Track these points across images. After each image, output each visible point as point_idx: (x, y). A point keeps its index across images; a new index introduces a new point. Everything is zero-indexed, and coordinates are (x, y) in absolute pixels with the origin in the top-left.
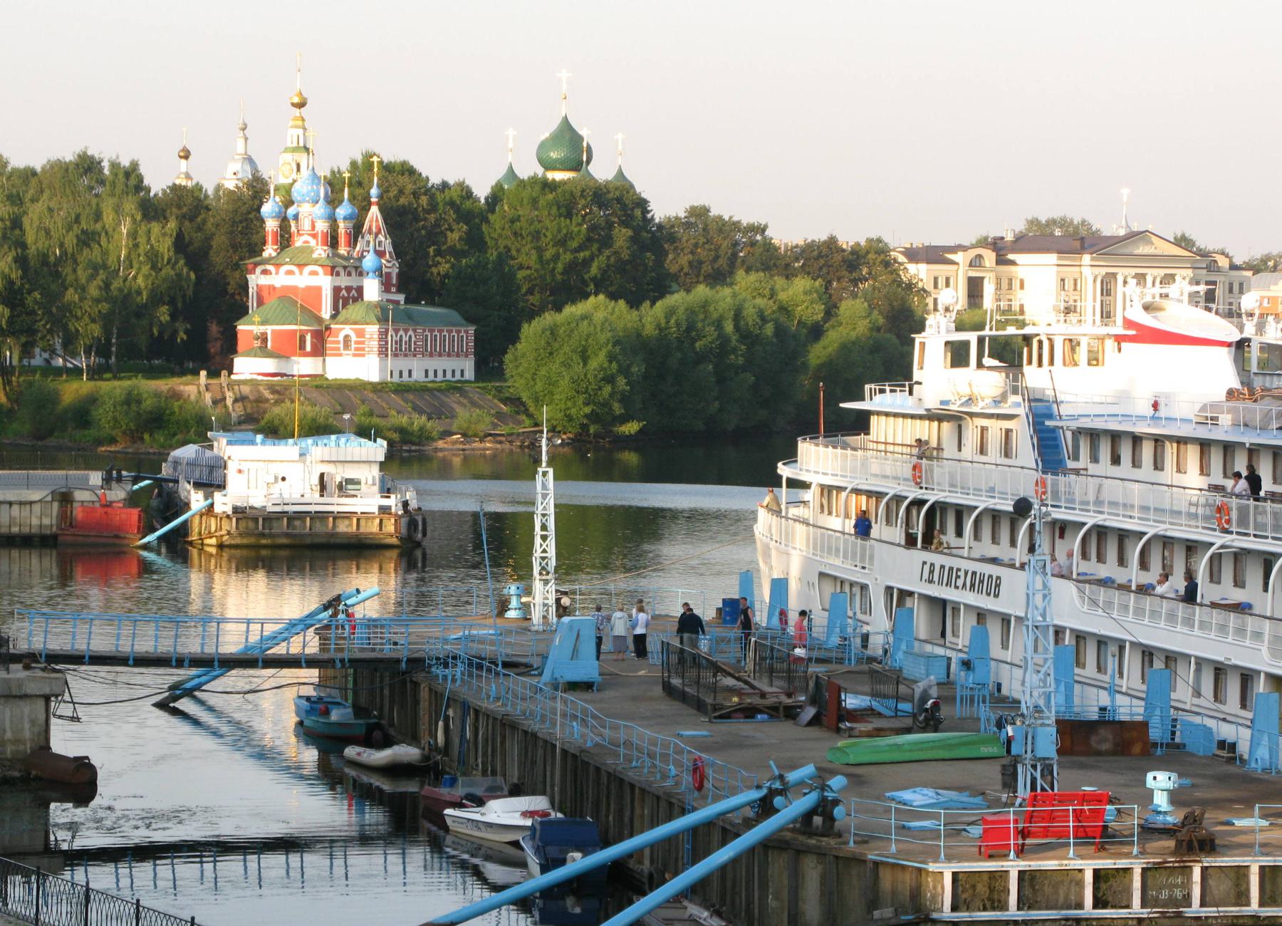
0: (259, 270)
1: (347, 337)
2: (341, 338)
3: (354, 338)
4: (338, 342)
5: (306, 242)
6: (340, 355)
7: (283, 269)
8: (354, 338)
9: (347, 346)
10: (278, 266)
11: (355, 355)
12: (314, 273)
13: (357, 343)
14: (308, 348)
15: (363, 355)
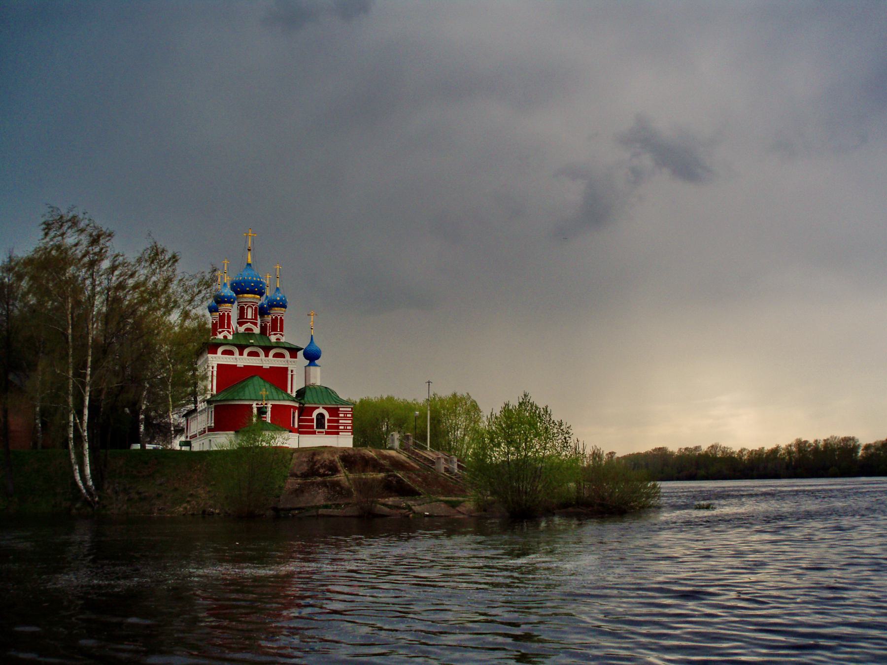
0: (220, 350)
1: (321, 416)
2: (314, 416)
3: (327, 416)
4: (312, 421)
5: (247, 329)
6: (314, 433)
7: (246, 352)
8: (327, 416)
9: (320, 424)
10: (241, 349)
11: (327, 433)
12: (282, 356)
13: (329, 421)
14: (296, 426)
15: (337, 433)
